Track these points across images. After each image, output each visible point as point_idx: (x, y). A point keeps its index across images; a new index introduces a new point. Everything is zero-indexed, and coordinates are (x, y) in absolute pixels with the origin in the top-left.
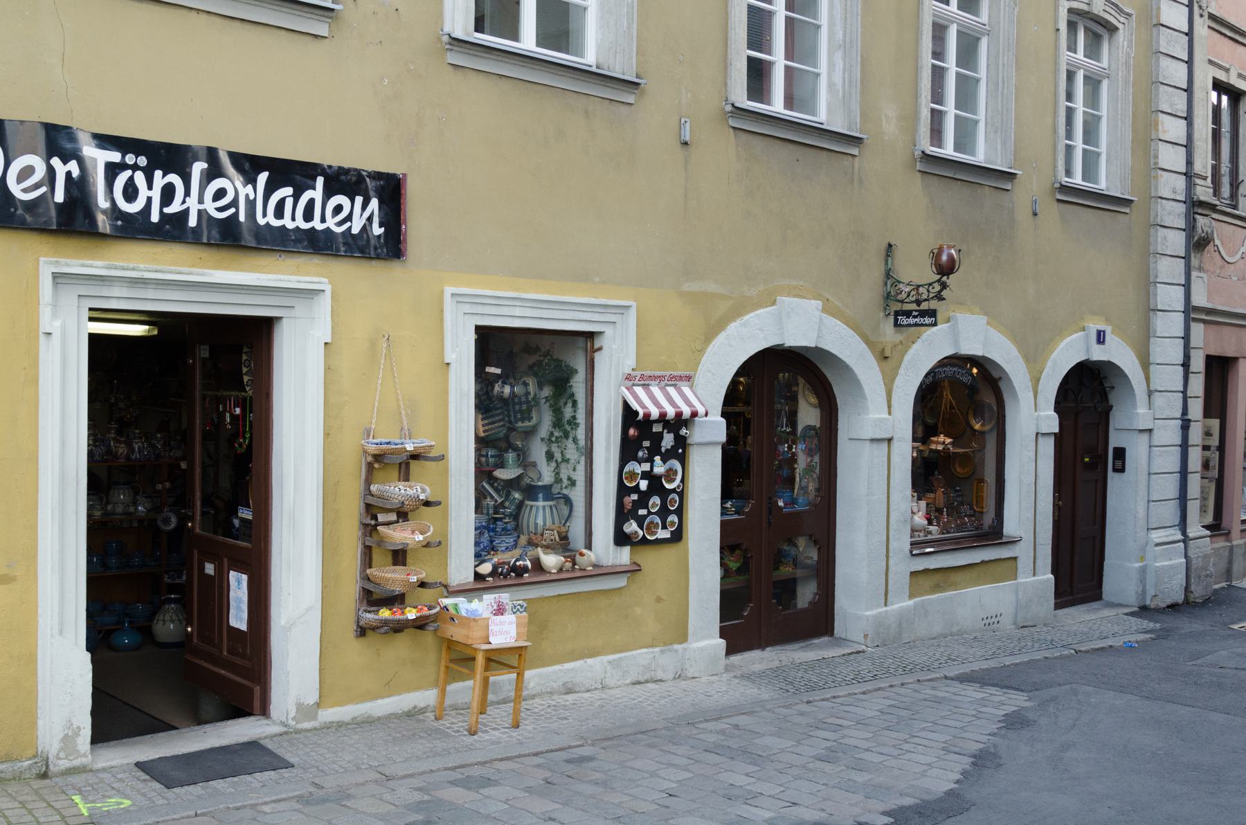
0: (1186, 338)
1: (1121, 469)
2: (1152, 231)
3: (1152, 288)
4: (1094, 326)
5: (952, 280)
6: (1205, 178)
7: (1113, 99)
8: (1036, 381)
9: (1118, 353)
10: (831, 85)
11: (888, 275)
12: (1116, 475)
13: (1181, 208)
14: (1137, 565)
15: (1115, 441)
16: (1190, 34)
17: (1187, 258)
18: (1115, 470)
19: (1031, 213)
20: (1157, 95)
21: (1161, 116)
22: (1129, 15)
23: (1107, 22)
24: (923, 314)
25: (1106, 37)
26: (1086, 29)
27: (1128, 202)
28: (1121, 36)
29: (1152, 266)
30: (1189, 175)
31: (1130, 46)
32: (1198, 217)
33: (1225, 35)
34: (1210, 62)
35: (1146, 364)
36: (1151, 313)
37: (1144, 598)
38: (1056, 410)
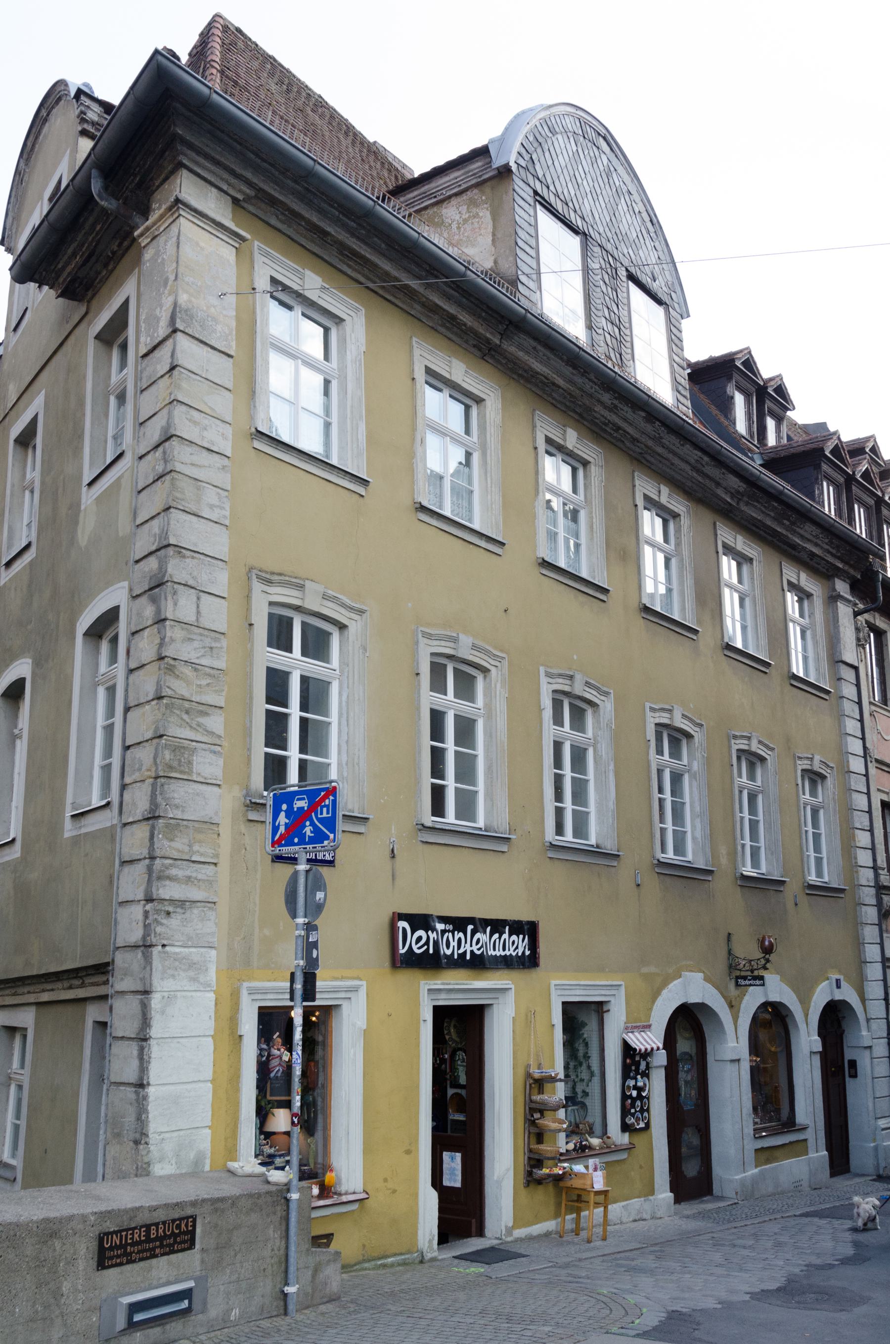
1: (854, 1075)
2: (858, 908)
3: (861, 947)
4: (834, 976)
5: (772, 957)
6: (883, 869)
7: (827, 822)
8: (806, 1015)
9: (848, 994)
10: (694, 839)
11: (730, 952)
12: (851, 1079)
13: (872, 891)
14: (872, 1145)
15: (849, 1055)
16: (866, 775)
17: (880, 925)
18: (850, 1076)
20: (852, 818)
21: (857, 831)
22: (832, 768)
24: (755, 978)
25: (819, 781)
27: (842, 891)
28: (829, 782)
29: (860, 931)
30: (875, 868)
31: (834, 787)
32: (883, 896)
34: (879, 790)
35: (863, 1000)
37: (878, 1169)
38: (819, 1036)
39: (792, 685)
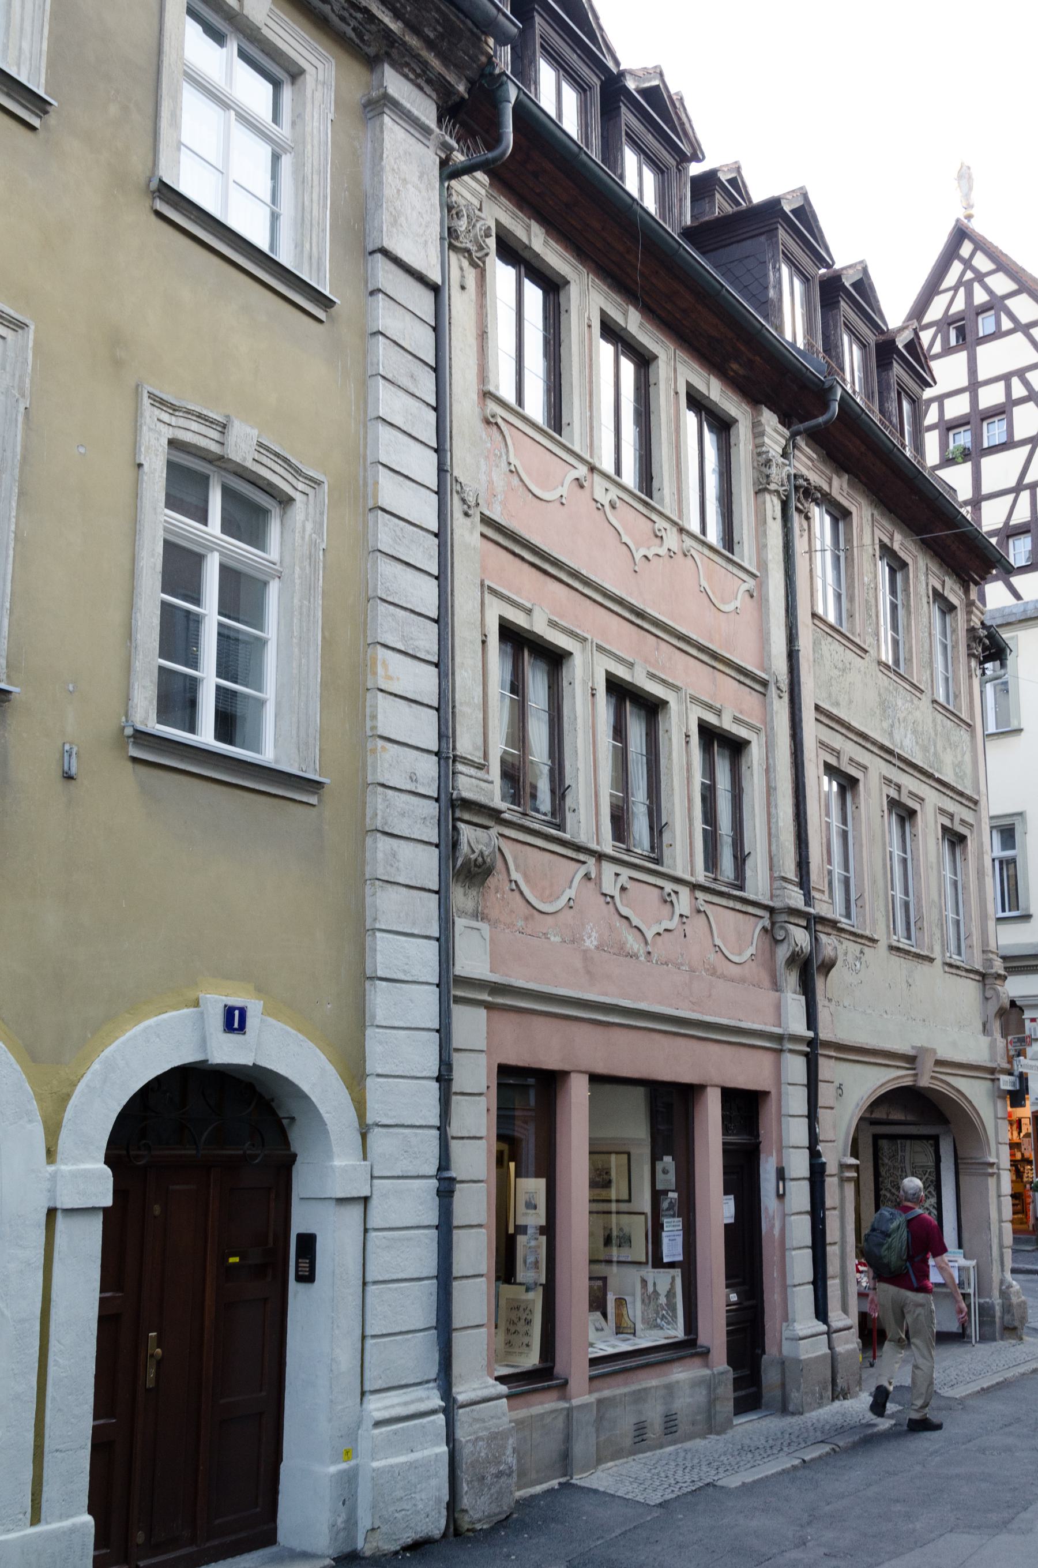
0: (444, 1031)
1: (308, 1277)
2: (369, 840)
3: (368, 939)
4: (215, 1003)
12: (302, 1287)
13: (431, 809)
14: (333, 1469)
15: (299, 1225)
17: (441, 893)
18: (300, 1279)
19: (56, 773)
20: (375, 617)
21: (381, 651)
23: (270, 484)
25: (276, 511)
26: (227, 492)
27: (314, 786)
28: (299, 510)
29: (368, 900)
31: (318, 528)
32: (461, 826)
33: (523, 559)
36: (368, 983)
37: (351, 1537)
38: (108, 1161)
39: (159, 214)
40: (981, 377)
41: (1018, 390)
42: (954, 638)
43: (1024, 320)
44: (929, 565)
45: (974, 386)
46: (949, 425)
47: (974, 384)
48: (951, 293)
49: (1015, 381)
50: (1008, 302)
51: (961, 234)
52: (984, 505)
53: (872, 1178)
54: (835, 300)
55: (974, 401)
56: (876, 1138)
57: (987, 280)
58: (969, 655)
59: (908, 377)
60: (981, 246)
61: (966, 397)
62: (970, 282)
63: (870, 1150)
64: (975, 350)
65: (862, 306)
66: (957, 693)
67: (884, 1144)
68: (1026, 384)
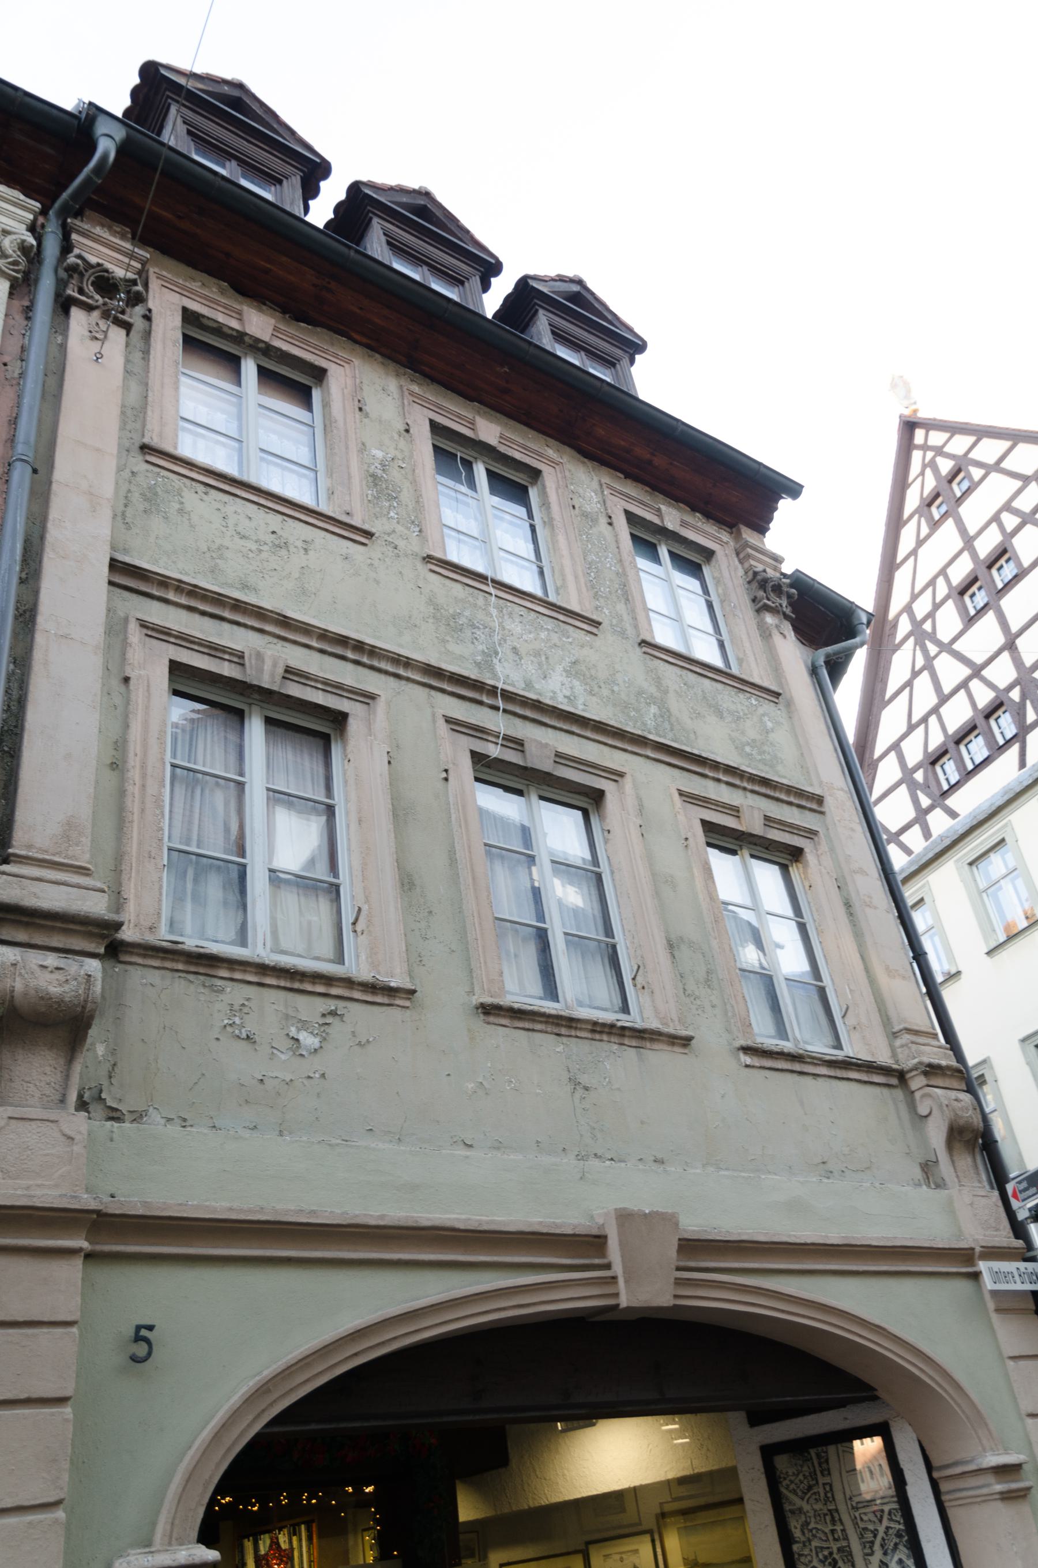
40: (972, 532)
41: (1010, 521)
42: (720, 591)
43: (991, 460)
44: (603, 481)
45: (969, 543)
46: (959, 589)
47: (968, 541)
48: (920, 478)
49: (1005, 517)
50: (971, 455)
51: (909, 426)
52: (1019, 642)
53: (777, 1548)
54: (368, 218)
55: (974, 555)
56: (769, 1452)
57: (946, 449)
58: (758, 611)
59: (586, 334)
60: (930, 425)
61: (966, 555)
62: (933, 461)
63: (763, 1484)
64: (958, 513)
65: (436, 232)
66: (741, 656)
67: (782, 1462)
68: (1016, 512)
